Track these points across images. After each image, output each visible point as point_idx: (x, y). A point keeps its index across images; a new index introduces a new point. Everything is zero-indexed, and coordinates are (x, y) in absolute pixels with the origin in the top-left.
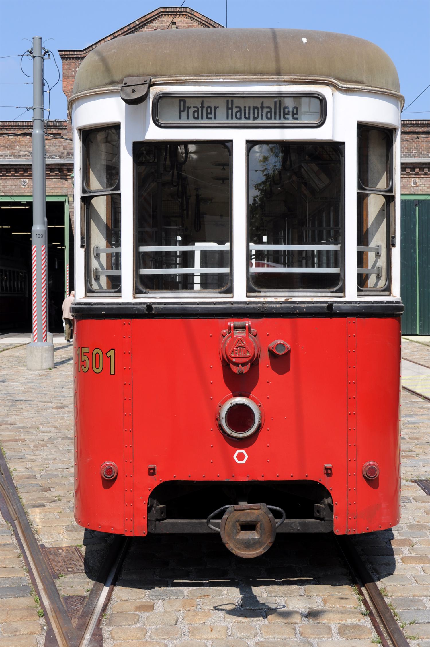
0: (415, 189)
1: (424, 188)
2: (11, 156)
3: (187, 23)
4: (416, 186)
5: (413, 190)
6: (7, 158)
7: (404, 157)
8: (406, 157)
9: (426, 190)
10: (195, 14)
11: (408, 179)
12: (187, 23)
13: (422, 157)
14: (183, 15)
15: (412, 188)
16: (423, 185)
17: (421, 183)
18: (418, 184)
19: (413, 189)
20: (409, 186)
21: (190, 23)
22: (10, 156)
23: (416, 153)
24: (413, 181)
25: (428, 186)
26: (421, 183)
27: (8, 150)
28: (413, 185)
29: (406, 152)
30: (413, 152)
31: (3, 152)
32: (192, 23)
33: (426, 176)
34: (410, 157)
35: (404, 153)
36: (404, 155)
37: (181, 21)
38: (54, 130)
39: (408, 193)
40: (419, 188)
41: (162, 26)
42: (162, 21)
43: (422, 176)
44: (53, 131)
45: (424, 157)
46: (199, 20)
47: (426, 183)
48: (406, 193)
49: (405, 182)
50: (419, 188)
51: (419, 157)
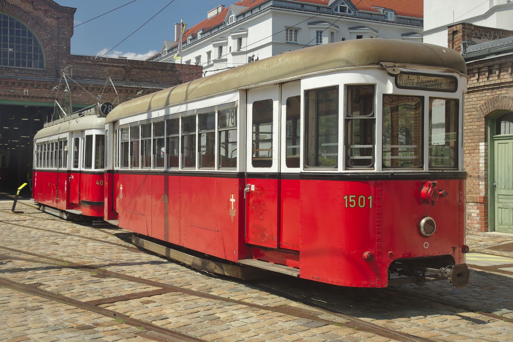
29: (149, 82)
30: (153, 82)
35: (148, 82)
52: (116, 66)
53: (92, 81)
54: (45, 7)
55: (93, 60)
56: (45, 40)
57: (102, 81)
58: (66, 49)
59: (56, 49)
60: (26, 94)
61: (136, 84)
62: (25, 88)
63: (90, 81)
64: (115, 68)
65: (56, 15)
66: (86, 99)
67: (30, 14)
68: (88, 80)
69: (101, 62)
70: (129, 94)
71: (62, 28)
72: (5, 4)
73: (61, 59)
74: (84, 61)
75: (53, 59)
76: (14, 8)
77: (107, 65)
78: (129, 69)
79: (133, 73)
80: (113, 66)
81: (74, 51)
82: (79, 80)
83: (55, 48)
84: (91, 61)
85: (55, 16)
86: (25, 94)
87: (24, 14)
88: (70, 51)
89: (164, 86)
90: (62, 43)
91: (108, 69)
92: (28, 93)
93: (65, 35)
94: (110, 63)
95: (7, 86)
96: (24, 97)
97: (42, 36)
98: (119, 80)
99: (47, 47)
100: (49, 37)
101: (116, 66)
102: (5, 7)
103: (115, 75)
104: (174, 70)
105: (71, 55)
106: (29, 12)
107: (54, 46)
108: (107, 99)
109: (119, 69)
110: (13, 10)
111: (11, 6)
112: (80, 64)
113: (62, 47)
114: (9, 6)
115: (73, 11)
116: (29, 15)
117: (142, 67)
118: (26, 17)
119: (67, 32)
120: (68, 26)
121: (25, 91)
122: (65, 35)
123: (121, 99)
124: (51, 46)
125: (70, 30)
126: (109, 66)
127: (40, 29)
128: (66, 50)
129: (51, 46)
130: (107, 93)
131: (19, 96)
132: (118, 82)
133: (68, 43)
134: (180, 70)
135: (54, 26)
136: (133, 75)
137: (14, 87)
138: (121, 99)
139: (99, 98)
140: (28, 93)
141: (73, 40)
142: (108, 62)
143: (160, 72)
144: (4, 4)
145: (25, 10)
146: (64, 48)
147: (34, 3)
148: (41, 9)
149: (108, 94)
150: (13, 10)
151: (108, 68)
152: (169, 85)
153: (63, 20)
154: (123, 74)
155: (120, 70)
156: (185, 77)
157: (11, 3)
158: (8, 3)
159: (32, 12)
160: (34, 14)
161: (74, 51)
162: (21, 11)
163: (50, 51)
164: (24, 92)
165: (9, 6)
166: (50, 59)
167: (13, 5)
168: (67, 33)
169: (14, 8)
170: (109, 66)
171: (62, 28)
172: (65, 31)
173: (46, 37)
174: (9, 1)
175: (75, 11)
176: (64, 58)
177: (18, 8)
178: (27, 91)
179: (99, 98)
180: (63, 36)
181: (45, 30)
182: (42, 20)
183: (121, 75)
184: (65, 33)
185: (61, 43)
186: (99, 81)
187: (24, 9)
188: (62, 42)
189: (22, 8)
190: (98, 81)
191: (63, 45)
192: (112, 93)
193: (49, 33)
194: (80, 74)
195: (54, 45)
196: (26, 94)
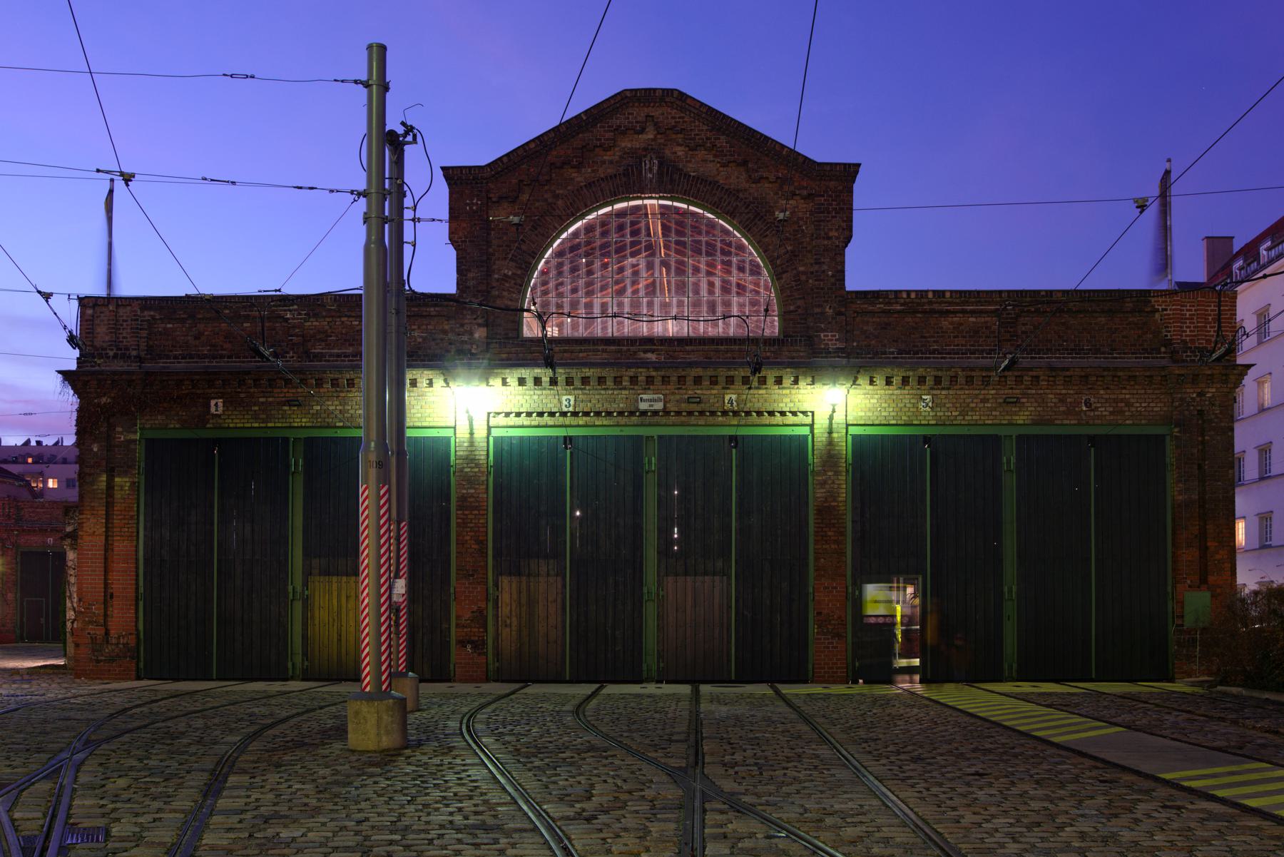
0: (1089, 416)
1: (1104, 413)
2: (356, 356)
3: (673, 118)
4: (1091, 411)
5: (1084, 418)
6: (349, 361)
7: (1068, 358)
8: (1072, 358)
9: (1108, 418)
10: (688, 101)
11: (1076, 396)
12: (673, 118)
13: (1100, 358)
14: (666, 102)
15: (1082, 414)
16: (1103, 409)
17: (1099, 405)
18: (1093, 407)
19: (1085, 415)
20: (1077, 409)
21: (679, 118)
22: (353, 356)
23: (1090, 350)
24: (1086, 401)
25: (1111, 409)
26: (1099, 405)
27: (350, 345)
28: (1084, 408)
30: (1083, 349)
31: (340, 349)
32: (683, 118)
33: (1109, 391)
34: (1080, 358)
35: (1067, 350)
36: (1068, 354)
37: (663, 114)
38: (432, 309)
39: (1076, 422)
40: (1096, 413)
41: (629, 122)
42: (629, 114)
43: (1102, 392)
44: (430, 312)
45: (1105, 358)
46: (696, 112)
47: (1108, 405)
48: (1072, 422)
49: (1070, 403)
50: (1096, 413)
51: (1096, 358)
52: (973, 312)
53: (905, 358)
54: (778, 172)
55: (908, 300)
56: (778, 258)
57: (934, 358)
58: (833, 276)
59: (807, 281)
60: (732, 406)
61: (1032, 358)
62: (728, 391)
63: (902, 358)
64: (971, 319)
65: (806, 188)
66: (891, 409)
67: (741, 195)
68: (894, 358)
69: (930, 303)
70: (1012, 389)
71: (823, 221)
72: (680, 178)
73: (819, 306)
74: (882, 306)
75: (799, 307)
76: (701, 184)
77: (948, 312)
78: (1011, 318)
79: (1023, 329)
80: (964, 312)
81: (854, 282)
82: (869, 358)
83: (803, 278)
84: (902, 305)
85: (805, 193)
86: (727, 406)
87: (726, 196)
88: (843, 280)
89: (1116, 358)
90: (824, 263)
91: (952, 323)
92: (735, 404)
93: (829, 238)
94: (957, 304)
95: (683, 387)
96: (725, 413)
97: (770, 247)
98: (982, 351)
99: (784, 276)
100: (789, 248)
101: (973, 312)
102: (678, 185)
103: (970, 337)
104: (1149, 309)
105: (849, 292)
106: (738, 191)
107: (804, 273)
108: (947, 406)
109: (983, 320)
110: (698, 191)
111: (693, 181)
112: (872, 312)
113: (824, 271)
114: (688, 181)
115: (849, 172)
116: (738, 197)
117: (1048, 310)
118: (729, 203)
119: (837, 230)
120: (839, 213)
121: (727, 398)
122: (829, 238)
123: (989, 405)
124: (795, 272)
125: (844, 225)
126: (954, 312)
127: (766, 230)
128: (833, 280)
129: (795, 272)
130: (948, 389)
131: (713, 413)
132: (979, 358)
133: (839, 259)
134: (1166, 310)
135: (802, 219)
136: (1023, 332)
137: (702, 389)
138: (989, 405)
139: (927, 405)
140: (735, 404)
141: (851, 253)
142: (950, 304)
143: (1103, 319)
144: (676, 177)
145: (726, 187)
146: (828, 275)
147: (750, 165)
148: (767, 178)
149: (951, 392)
150: (698, 191)
151: (950, 319)
152: (1133, 353)
153: (825, 200)
154: (994, 332)
155: (986, 322)
156: (1181, 327)
157: (692, 174)
158: (685, 175)
159: (746, 190)
160: (750, 194)
161: (854, 282)
162: (717, 190)
163: (792, 287)
164: (726, 401)
165: (688, 181)
166: (792, 308)
167: (698, 178)
168: (836, 234)
169: (701, 184)
170: (954, 312)
171: (823, 221)
172: (831, 230)
173: (782, 251)
174: (689, 169)
175: (857, 172)
176: (827, 301)
177: (710, 183)
178: (734, 397)
179: (927, 405)
180: (826, 242)
181: (778, 231)
182: (770, 207)
183: (987, 337)
184: (831, 234)
185: (820, 263)
186: (926, 358)
187: (725, 184)
188: (822, 260)
189: (721, 182)
190: (922, 358)
191: (825, 267)
192: (961, 389)
193: (787, 239)
194: (873, 342)
195: (801, 269)
196: (732, 406)
